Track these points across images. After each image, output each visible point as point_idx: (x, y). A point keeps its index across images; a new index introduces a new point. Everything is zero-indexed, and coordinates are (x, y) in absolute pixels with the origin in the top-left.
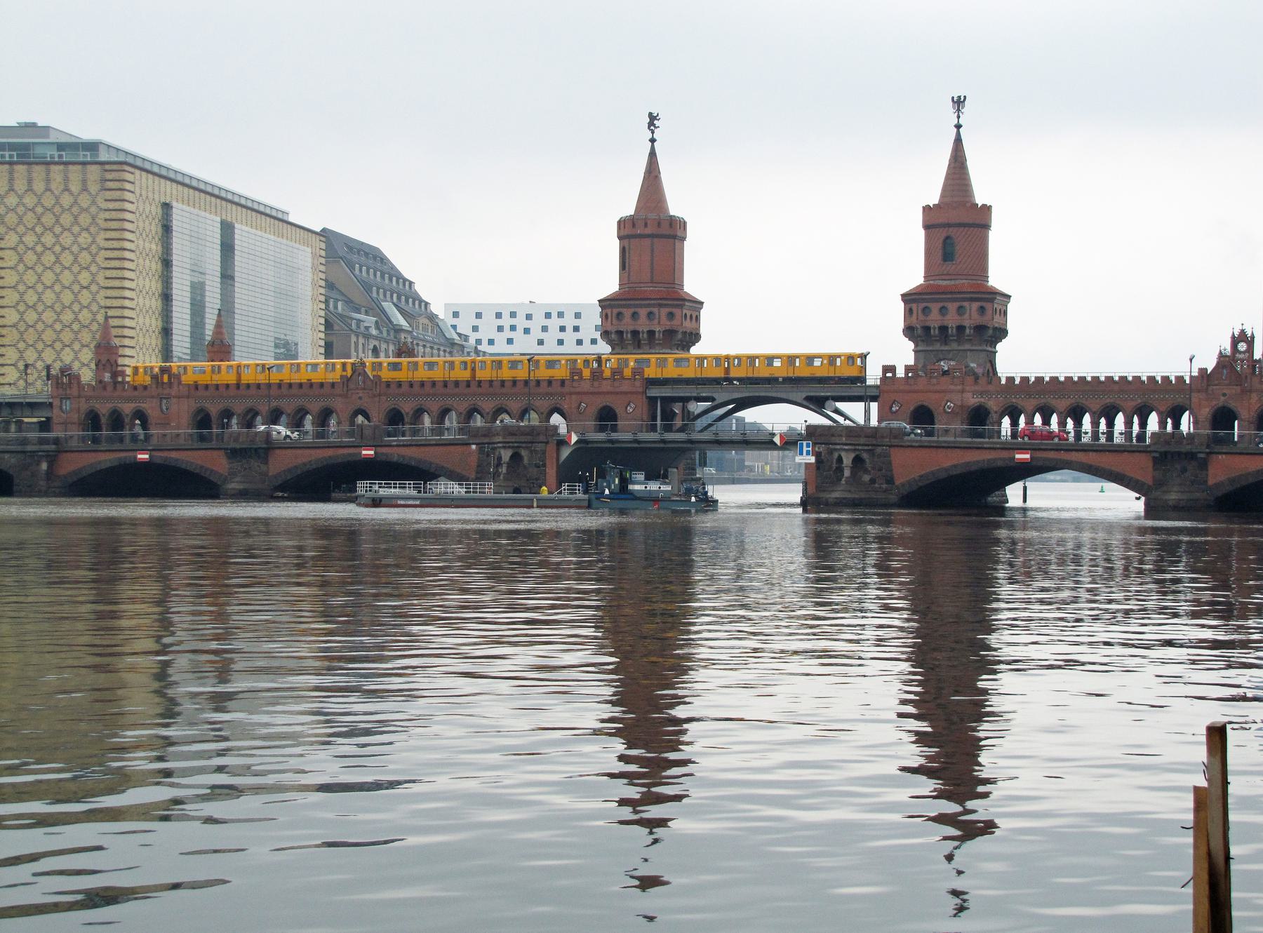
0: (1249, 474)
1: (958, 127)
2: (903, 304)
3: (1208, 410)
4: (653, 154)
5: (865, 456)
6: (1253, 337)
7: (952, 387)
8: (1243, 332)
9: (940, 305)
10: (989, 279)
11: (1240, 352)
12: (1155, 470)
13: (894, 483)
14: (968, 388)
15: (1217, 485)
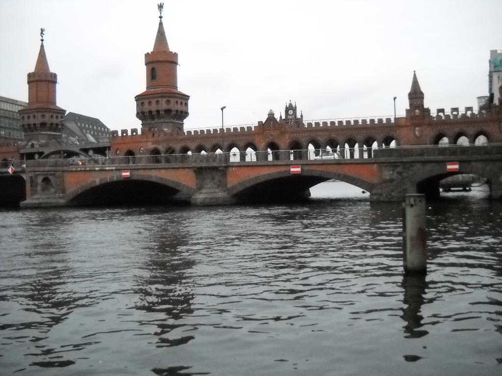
0: (251, 179)
1: (161, 17)
2: (135, 102)
3: (264, 144)
4: (42, 46)
5: (51, 178)
6: (296, 107)
7: (142, 140)
8: (290, 105)
9: (149, 101)
10: (178, 89)
11: (290, 115)
12: (197, 179)
13: (65, 193)
14: (150, 140)
15: (234, 187)
